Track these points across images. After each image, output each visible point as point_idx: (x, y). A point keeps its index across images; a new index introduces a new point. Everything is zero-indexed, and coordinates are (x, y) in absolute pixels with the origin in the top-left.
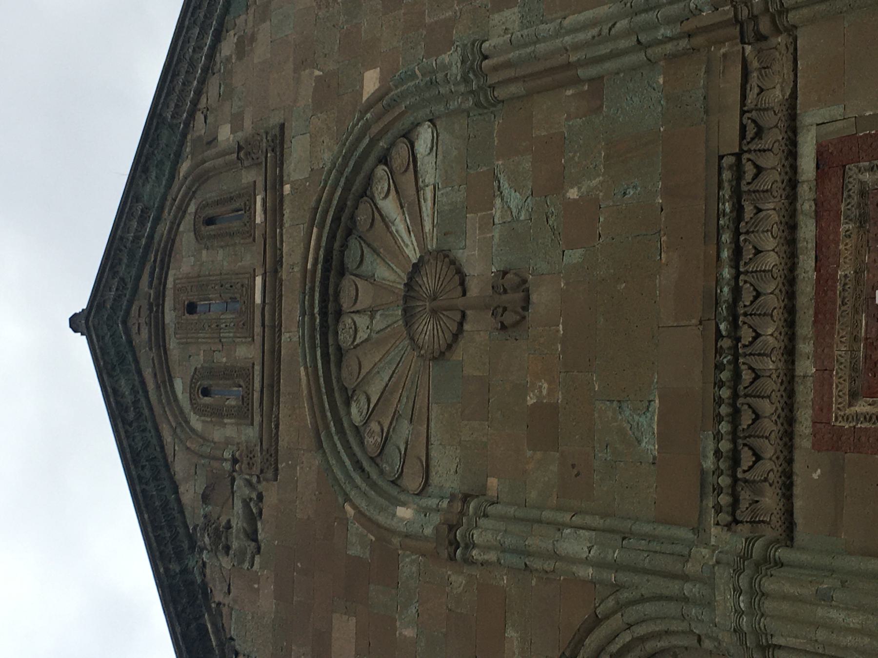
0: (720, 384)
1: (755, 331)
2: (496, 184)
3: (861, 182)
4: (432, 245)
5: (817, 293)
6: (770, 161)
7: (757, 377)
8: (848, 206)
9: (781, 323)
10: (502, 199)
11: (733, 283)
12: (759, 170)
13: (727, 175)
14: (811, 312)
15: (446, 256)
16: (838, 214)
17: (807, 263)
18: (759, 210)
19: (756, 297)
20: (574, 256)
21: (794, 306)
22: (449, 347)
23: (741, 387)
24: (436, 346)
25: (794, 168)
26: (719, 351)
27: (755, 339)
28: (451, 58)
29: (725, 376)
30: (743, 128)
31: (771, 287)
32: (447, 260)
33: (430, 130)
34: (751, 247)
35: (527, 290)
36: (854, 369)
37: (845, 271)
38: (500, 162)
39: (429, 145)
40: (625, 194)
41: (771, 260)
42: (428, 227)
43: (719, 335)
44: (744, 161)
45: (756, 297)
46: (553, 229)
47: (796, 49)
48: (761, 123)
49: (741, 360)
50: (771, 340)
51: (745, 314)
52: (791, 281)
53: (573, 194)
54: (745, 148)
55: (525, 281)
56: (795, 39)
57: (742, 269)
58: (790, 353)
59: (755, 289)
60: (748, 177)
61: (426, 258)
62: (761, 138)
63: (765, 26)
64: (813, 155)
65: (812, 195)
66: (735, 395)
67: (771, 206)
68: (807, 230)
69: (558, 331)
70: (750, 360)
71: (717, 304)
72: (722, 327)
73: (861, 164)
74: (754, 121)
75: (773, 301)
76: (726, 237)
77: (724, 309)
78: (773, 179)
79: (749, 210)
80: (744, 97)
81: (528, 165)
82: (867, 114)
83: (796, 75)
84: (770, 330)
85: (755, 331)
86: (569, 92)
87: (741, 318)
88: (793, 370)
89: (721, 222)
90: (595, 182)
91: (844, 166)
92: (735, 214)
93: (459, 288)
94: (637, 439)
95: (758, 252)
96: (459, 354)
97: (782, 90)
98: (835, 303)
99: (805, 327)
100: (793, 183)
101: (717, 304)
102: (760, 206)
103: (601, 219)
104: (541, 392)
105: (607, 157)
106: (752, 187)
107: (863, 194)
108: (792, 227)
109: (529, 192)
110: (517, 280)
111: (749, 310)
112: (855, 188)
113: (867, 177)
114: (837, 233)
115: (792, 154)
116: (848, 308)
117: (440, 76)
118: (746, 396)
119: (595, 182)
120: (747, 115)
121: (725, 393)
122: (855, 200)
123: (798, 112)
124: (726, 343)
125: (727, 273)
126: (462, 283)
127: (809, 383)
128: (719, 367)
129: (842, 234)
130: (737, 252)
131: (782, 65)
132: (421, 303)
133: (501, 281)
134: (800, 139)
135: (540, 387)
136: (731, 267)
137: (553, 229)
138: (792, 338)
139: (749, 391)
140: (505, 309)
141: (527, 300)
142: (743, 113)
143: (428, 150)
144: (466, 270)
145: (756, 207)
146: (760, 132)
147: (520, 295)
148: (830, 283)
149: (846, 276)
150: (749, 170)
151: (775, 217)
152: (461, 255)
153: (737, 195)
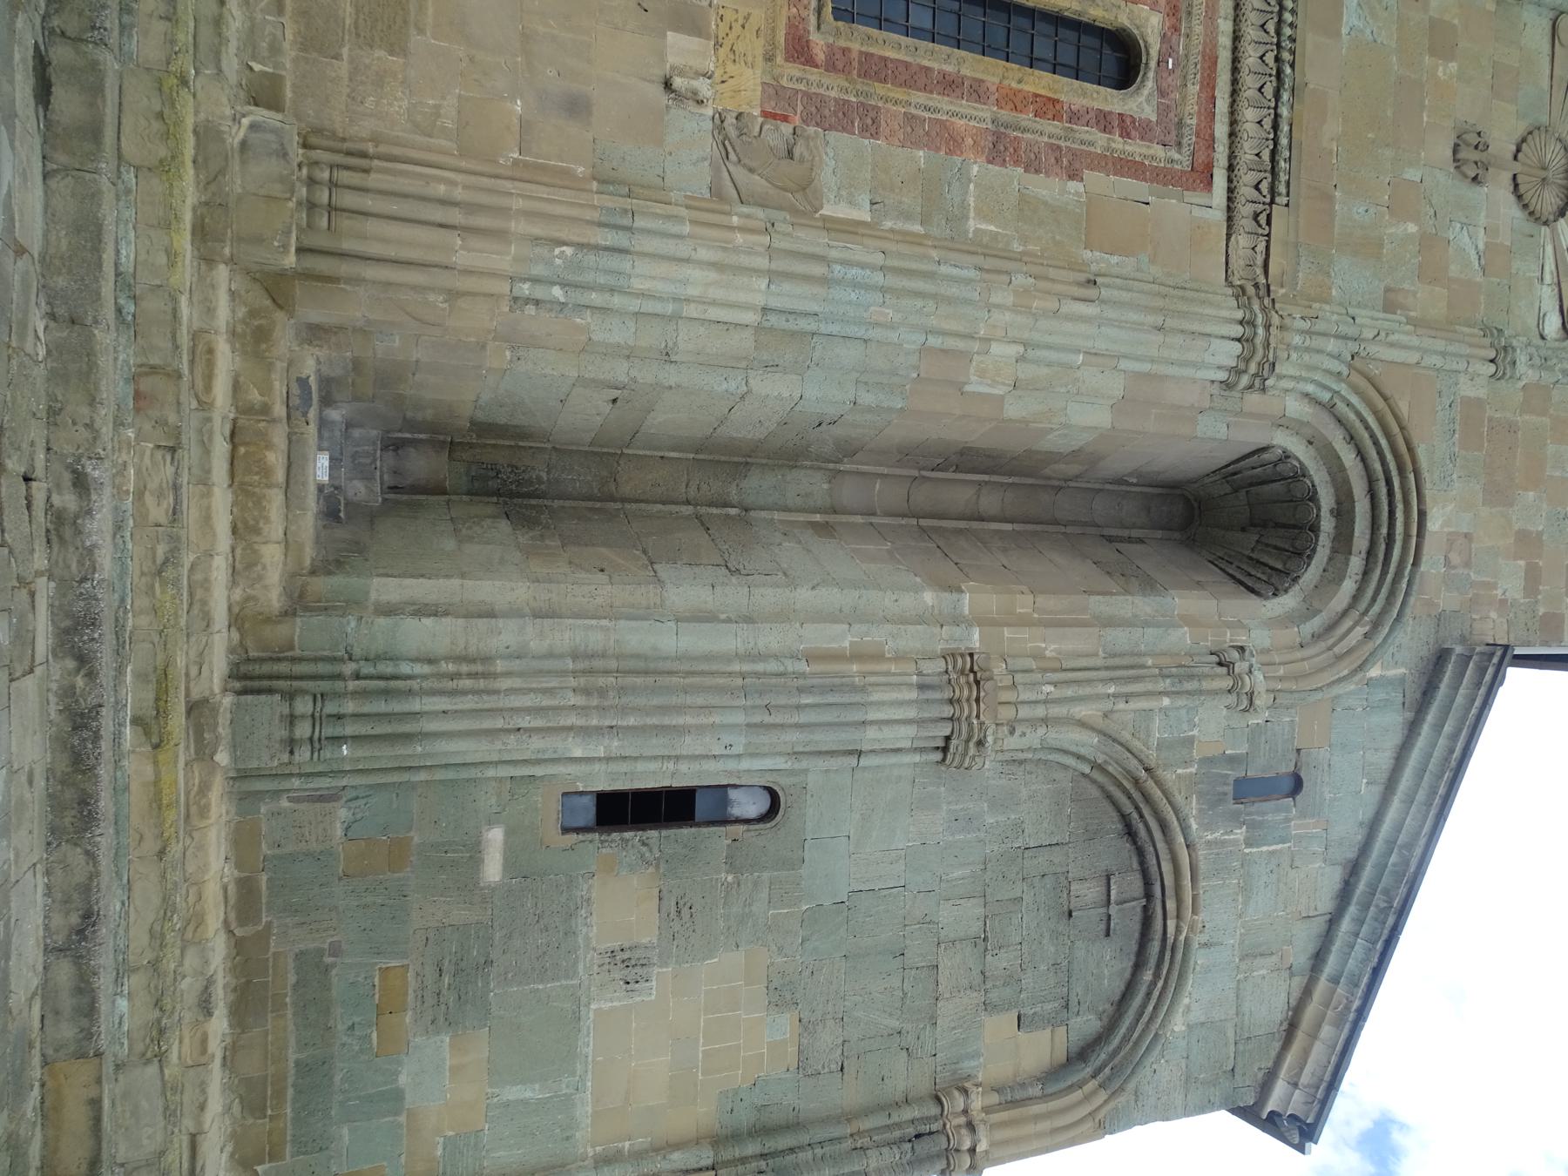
0: (1291, 25)
1: (1263, 61)
2: (1483, 262)
3: (1180, 153)
4: (1545, 230)
5: (1215, 79)
6: (1245, 192)
7: (1262, 26)
8: (1189, 139)
9: (1243, 60)
10: (1477, 247)
11: (1280, 104)
12: (1257, 187)
13: (1282, 189)
14: (1219, 66)
15: (1532, 213)
16: (1198, 136)
17: (1222, 105)
18: (1257, 155)
19: (1262, 87)
20: (1412, 174)
21: (1233, 74)
22: (1530, 133)
23: (1276, 20)
24: (1543, 137)
25: (1230, 180)
26: (1293, 52)
27: (1264, 55)
28: (1526, 372)
29: (1287, 31)
30: (1269, 223)
31: (1249, 93)
32: (1531, 209)
33: (1546, 332)
34: (1265, 127)
35: (1454, 160)
36: (1189, 13)
37: (1193, 89)
38: (1478, 279)
39: (1547, 319)
40: (1367, 211)
41: (1249, 115)
42: (1549, 249)
43: (1292, 66)
44: (1268, 196)
45: (1262, 87)
46: (1431, 205)
47: (1227, 271)
48: (1254, 223)
49: (1275, 40)
50: (1252, 54)
51: (1270, 75)
52: (1234, 93)
53: (1412, 228)
54: (1267, 207)
55: (1457, 167)
56: (1226, 279)
57: (1272, 111)
58: (1236, 38)
59: (1262, 93)
60: (1264, 182)
61: (1551, 218)
62: (1255, 212)
63: (1251, 290)
64: (1215, 186)
65: (1217, 156)
66: (1280, 14)
67: (1248, 156)
68: (1221, 130)
69: (1428, 117)
70: (1266, 38)
71: (1293, 90)
72: (1288, 70)
73: (1179, 167)
74: (1260, 226)
75: (1249, 82)
76: (1284, 141)
77: (1288, 84)
78: (1247, 178)
79: (1266, 155)
80: (1267, 248)
81: (1452, 267)
82: (1174, 201)
83: (1227, 252)
84: (1250, 58)
85: (1263, 61)
86: (1412, 314)
87: (1274, 73)
88: (1234, 26)
89: (1288, 154)
90: (1392, 230)
91: (1192, 170)
92: (1277, 158)
93: (1520, 179)
94: (1361, 8)
95: (1259, 122)
96: (1521, 129)
97: (1237, 242)
98: (1202, 68)
99: (1224, 57)
100: (1231, 168)
101: (1293, 90)
102: (1256, 158)
103: (1387, 197)
104: (1444, 70)
105: (1381, 246)
106: (1262, 175)
107: (1179, 144)
108: (1232, 134)
109: (1452, 243)
110: (1464, 168)
111: (1267, 78)
112: (1185, 150)
113: (1176, 156)
114: (1199, 119)
115: (1230, 190)
116: (1192, 60)
117: (1537, 361)
118: (1272, 12)
119: (1392, 230)
120: (1266, 232)
121: (1288, 17)
122: (1185, 141)
123: (1225, 223)
124: (1286, 56)
125: (1284, 111)
126: (1516, 186)
127: (1222, 13)
128: (1293, 40)
129: (1195, 117)
130: (1275, 127)
131: (1237, 263)
132: (1559, 181)
133: (1480, 172)
134: (1224, 200)
135: (1445, 74)
136: (1281, 117)
137: (1431, 205)
138: (1235, 49)
139: (1269, 16)
140: (1476, 147)
141: (1455, 151)
142: (1268, 235)
143: (1548, 315)
144: (1512, 198)
145: (1260, 158)
146: (1256, 216)
147: (1461, 155)
148: (1205, 83)
149: (1193, 84)
150: (1264, 186)
151: (1246, 146)
152: (1516, 212)
153: (1274, 172)
